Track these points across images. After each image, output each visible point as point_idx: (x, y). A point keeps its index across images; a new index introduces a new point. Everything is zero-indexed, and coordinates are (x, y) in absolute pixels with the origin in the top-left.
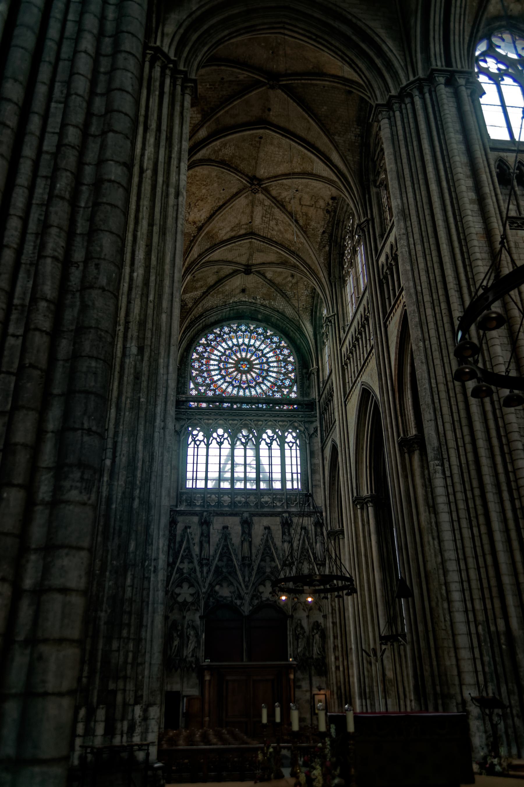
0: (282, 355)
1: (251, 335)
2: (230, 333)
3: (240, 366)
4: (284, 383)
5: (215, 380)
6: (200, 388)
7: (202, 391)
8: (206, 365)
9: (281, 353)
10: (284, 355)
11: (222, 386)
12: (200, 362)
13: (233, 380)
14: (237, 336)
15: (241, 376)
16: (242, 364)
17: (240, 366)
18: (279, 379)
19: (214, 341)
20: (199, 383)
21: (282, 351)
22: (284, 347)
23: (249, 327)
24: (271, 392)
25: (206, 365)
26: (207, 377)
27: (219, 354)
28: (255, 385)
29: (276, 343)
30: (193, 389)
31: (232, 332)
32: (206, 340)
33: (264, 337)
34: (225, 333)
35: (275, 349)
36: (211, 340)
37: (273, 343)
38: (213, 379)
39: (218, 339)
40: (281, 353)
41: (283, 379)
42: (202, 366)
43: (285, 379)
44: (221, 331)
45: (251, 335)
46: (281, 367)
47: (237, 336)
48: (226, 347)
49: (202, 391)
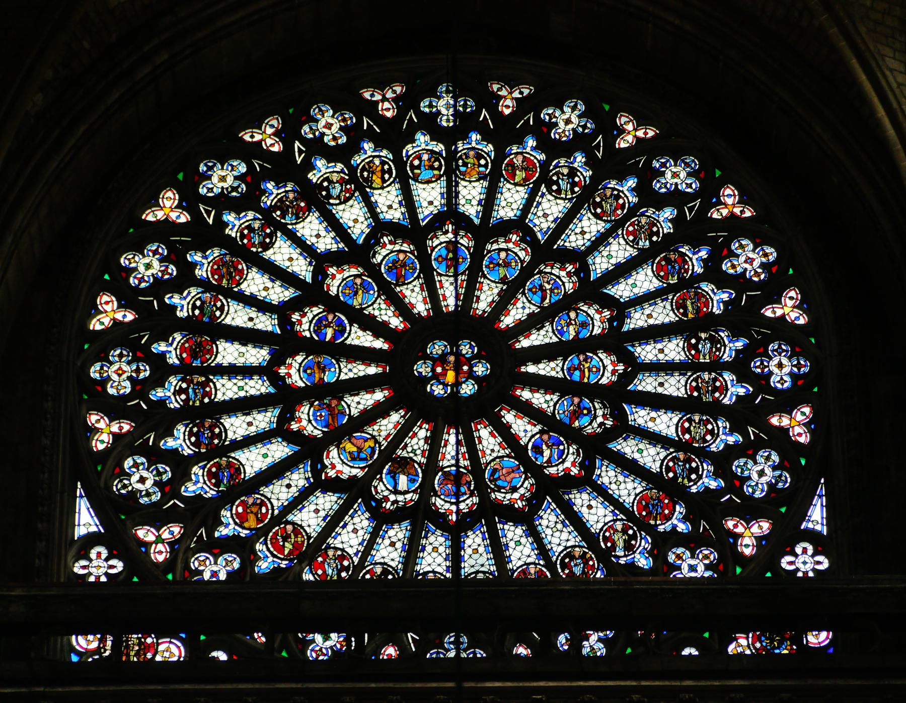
0: (722, 281)
1: (501, 155)
2: (353, 147)
3: (423, 369)
4: (736, 483)
5: (250, 471)
6: (145, 534)
7: (160, 554)
8: (184, 370)
9: (713, 273)
10: (739, 282)
11: (296, 517)
12: (141, 354)
13: (374, 471)
14: (400, 162)
15: (435, 443)
16: (441, 360)
17: (423, 369)
18: (704, 454)
19: (239, 206)
20: (134, 494)
21: (720, 252)
22: (734, 226)
23: (491, 101)
24: (644, 543)
25: (184, 370)
26: (196, 459)
27: (278, 294)
28: (535, 503)
29: (676, 198)
30: (91, 540)
31: (370, 135)
32: (189, 200)
33: (591, 162)
34: (317, 147)
35: (669, 243)
36: (223, 202)
37: (660, 201)
38: (236, 469)
39: (272, 193)
40: (713, 273)
41: (731, 452)
42: (158, 379)
43: (748, 450)
44: (287, 135)
45: (501, 155)
46: (716, 366)
47: (400, 162)
48: (327, 243)
49: (160, 554)
